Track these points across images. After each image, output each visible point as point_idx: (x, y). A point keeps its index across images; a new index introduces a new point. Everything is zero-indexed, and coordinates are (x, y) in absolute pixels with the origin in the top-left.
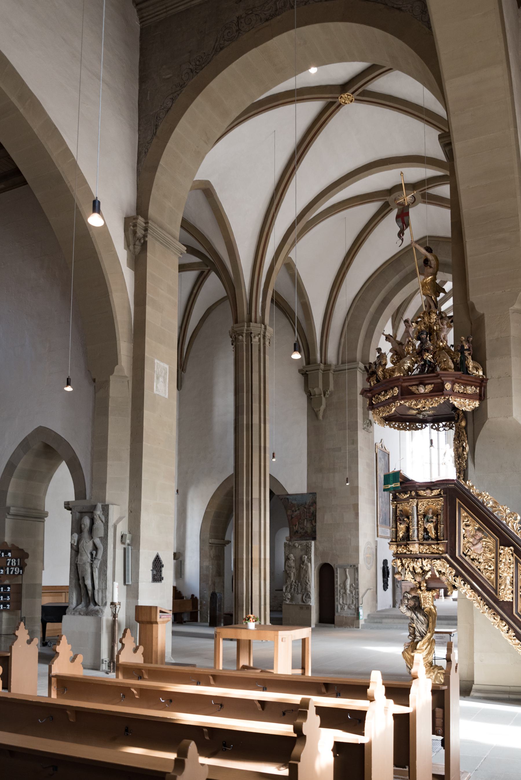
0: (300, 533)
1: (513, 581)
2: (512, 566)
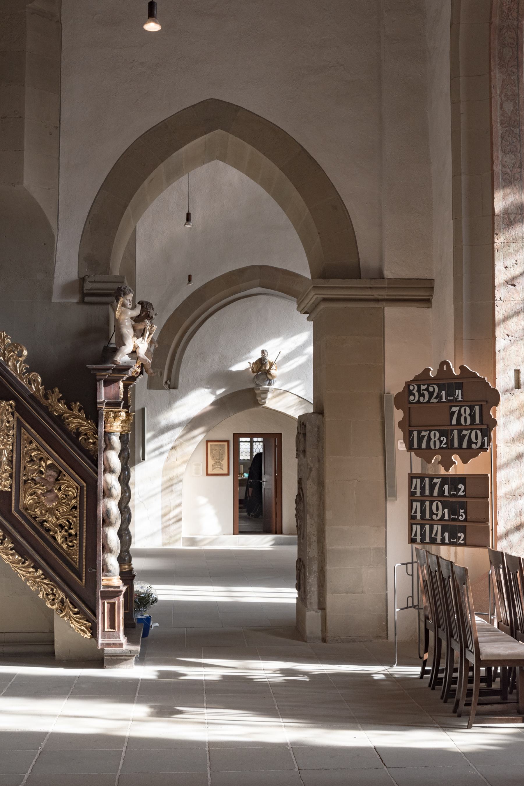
1: (12, 457)
2: (11, 432)
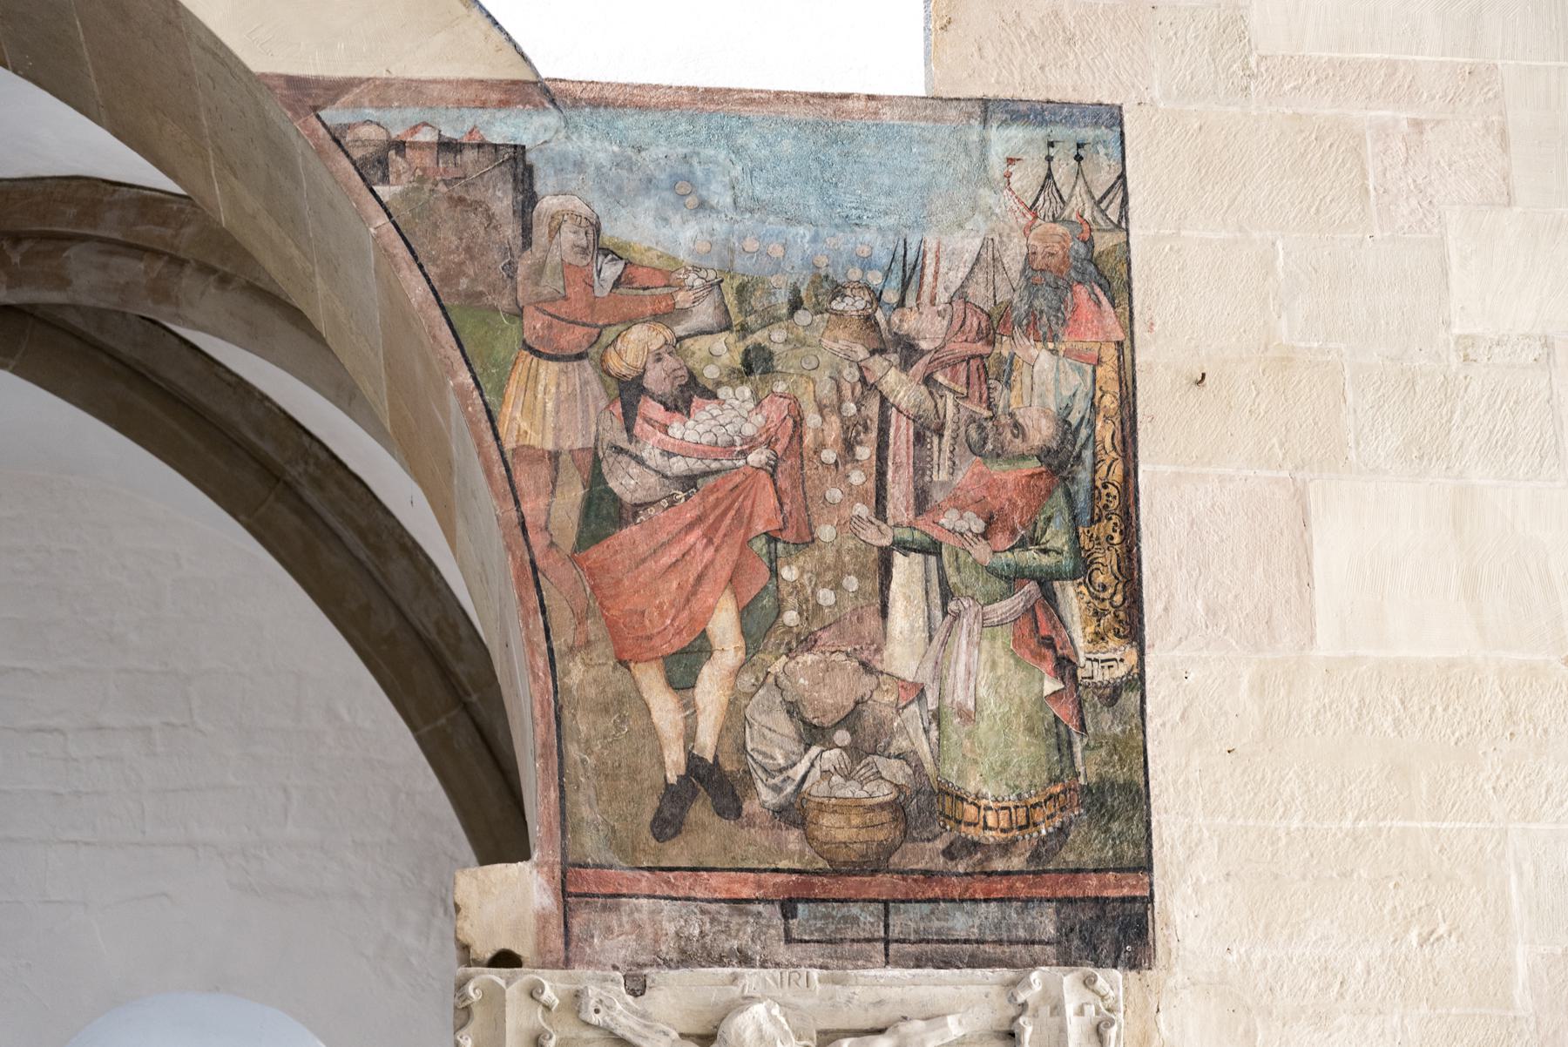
0: (794, 813)
